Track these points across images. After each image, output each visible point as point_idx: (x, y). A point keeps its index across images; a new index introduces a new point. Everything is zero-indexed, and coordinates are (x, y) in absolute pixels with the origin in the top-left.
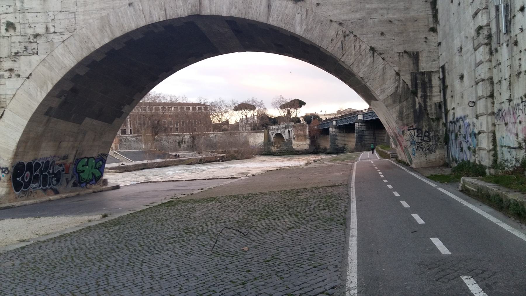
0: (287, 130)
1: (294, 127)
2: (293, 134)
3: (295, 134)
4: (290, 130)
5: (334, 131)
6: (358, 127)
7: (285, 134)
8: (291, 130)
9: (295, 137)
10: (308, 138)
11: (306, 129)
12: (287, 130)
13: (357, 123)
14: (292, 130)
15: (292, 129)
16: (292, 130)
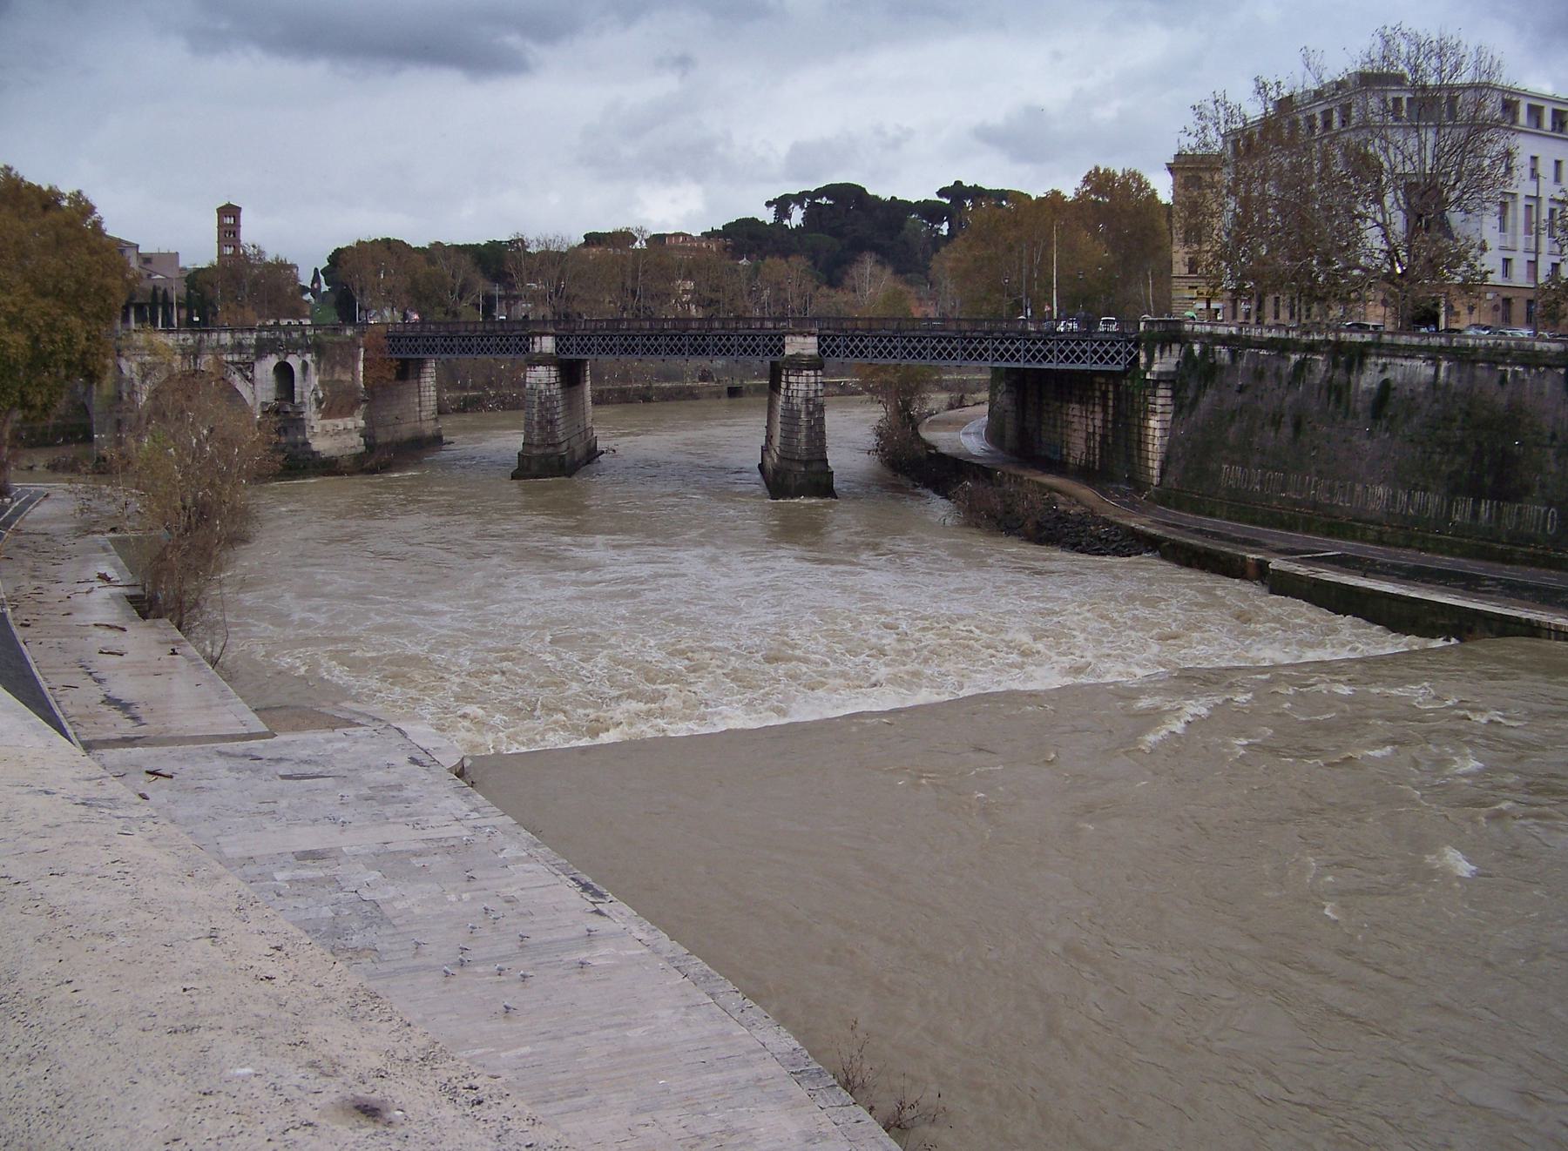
0: (272, 361)
1: (318, 348)
2: (309, 386)
3: (322, 383)
4: (294, 362)
5: (553, 380)
6: (813, 387)
7: (251, 381)
8: (305, 366)
9: (321, 395)
10: (364, 401)
11: (355, 358)
12: (272, 361)
13: (812, 373)
14: (312, 367)
15: (308, 357)
16: (312, 367)
